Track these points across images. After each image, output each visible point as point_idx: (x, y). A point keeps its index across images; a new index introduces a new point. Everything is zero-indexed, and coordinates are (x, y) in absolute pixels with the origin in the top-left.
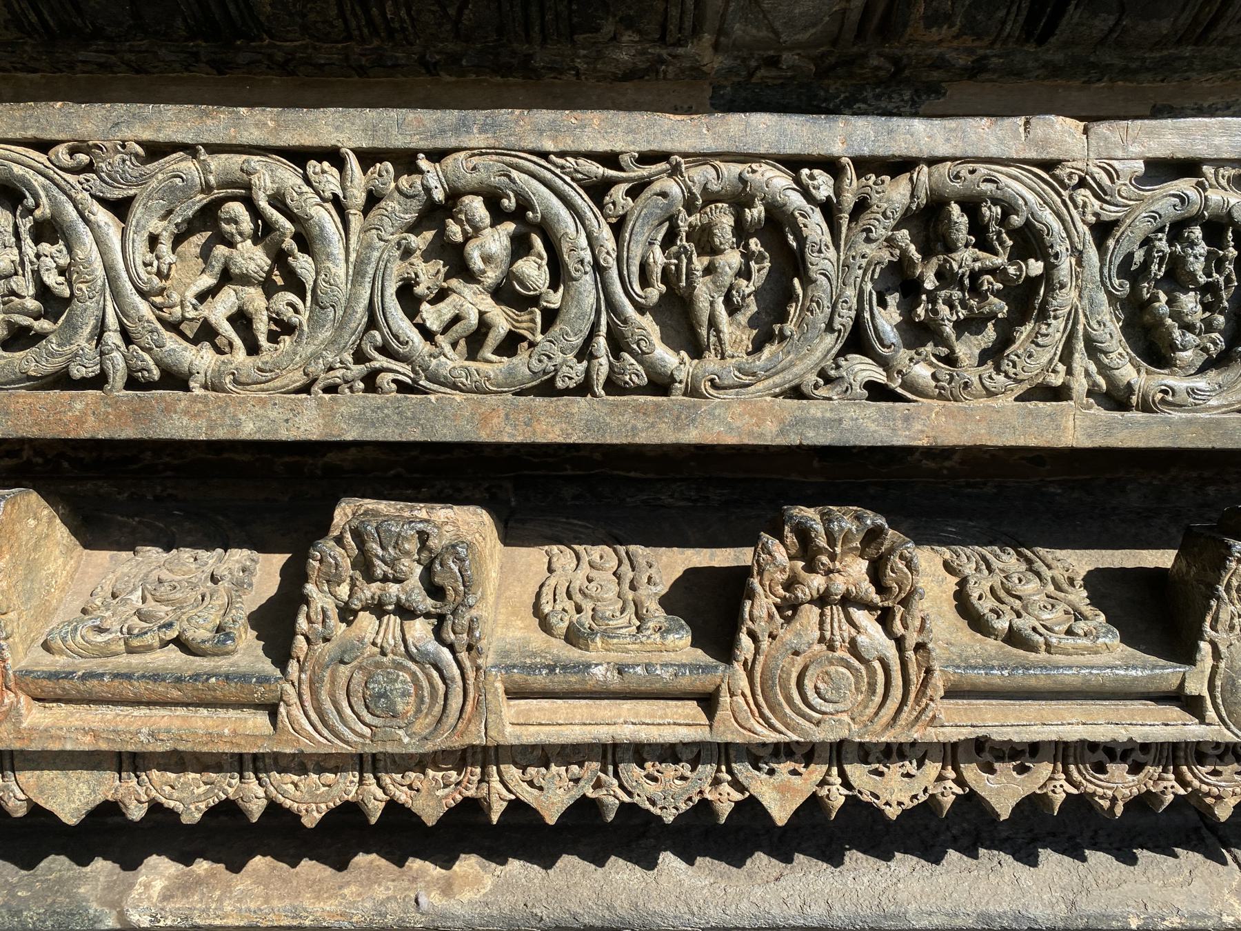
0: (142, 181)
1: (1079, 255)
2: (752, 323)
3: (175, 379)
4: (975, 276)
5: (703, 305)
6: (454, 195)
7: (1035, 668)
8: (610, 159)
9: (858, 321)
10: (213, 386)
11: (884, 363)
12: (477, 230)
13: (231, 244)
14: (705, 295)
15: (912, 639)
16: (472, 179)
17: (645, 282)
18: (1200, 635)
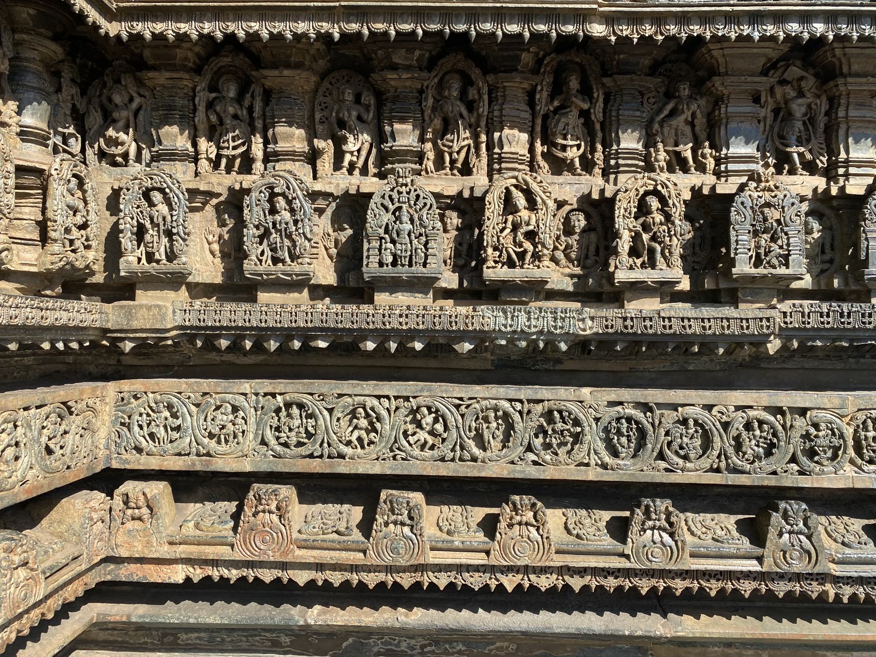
0: (337, 403)
1: (591, 426)
2: (502, 442)
3: (341, 456)
4: (562, 431)
5: (486, 437)
6: (418, 408)
7: (583, 545)
8: (461, 399)
9: (529, 443)
10: (351, 458)
11: (537, 455)
12: (425, 417)
13: (358, 419)
14: (487, 435)
15: (545, 536)
16: (424, 403)
17: (470, 431)
18: (626, 536)
